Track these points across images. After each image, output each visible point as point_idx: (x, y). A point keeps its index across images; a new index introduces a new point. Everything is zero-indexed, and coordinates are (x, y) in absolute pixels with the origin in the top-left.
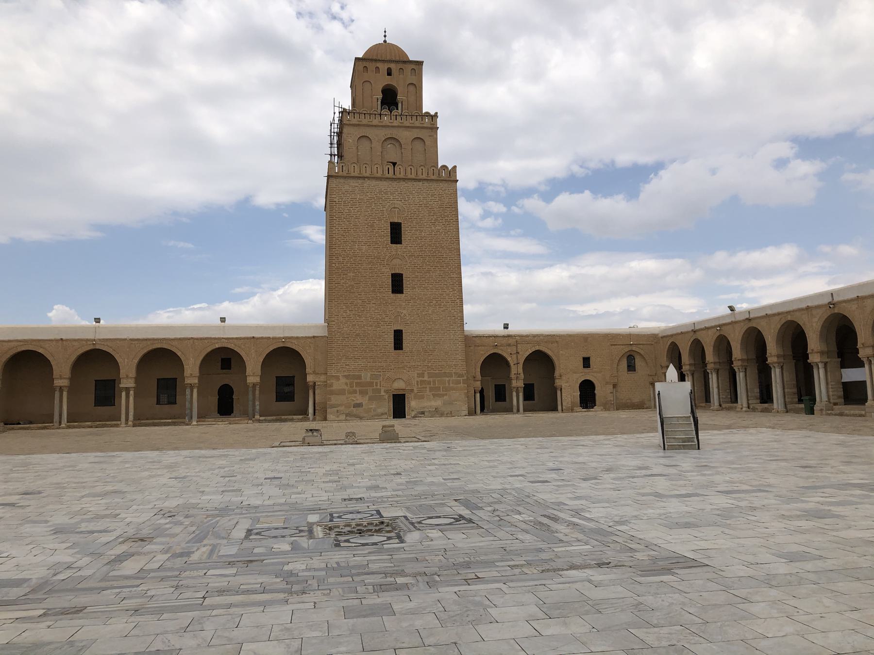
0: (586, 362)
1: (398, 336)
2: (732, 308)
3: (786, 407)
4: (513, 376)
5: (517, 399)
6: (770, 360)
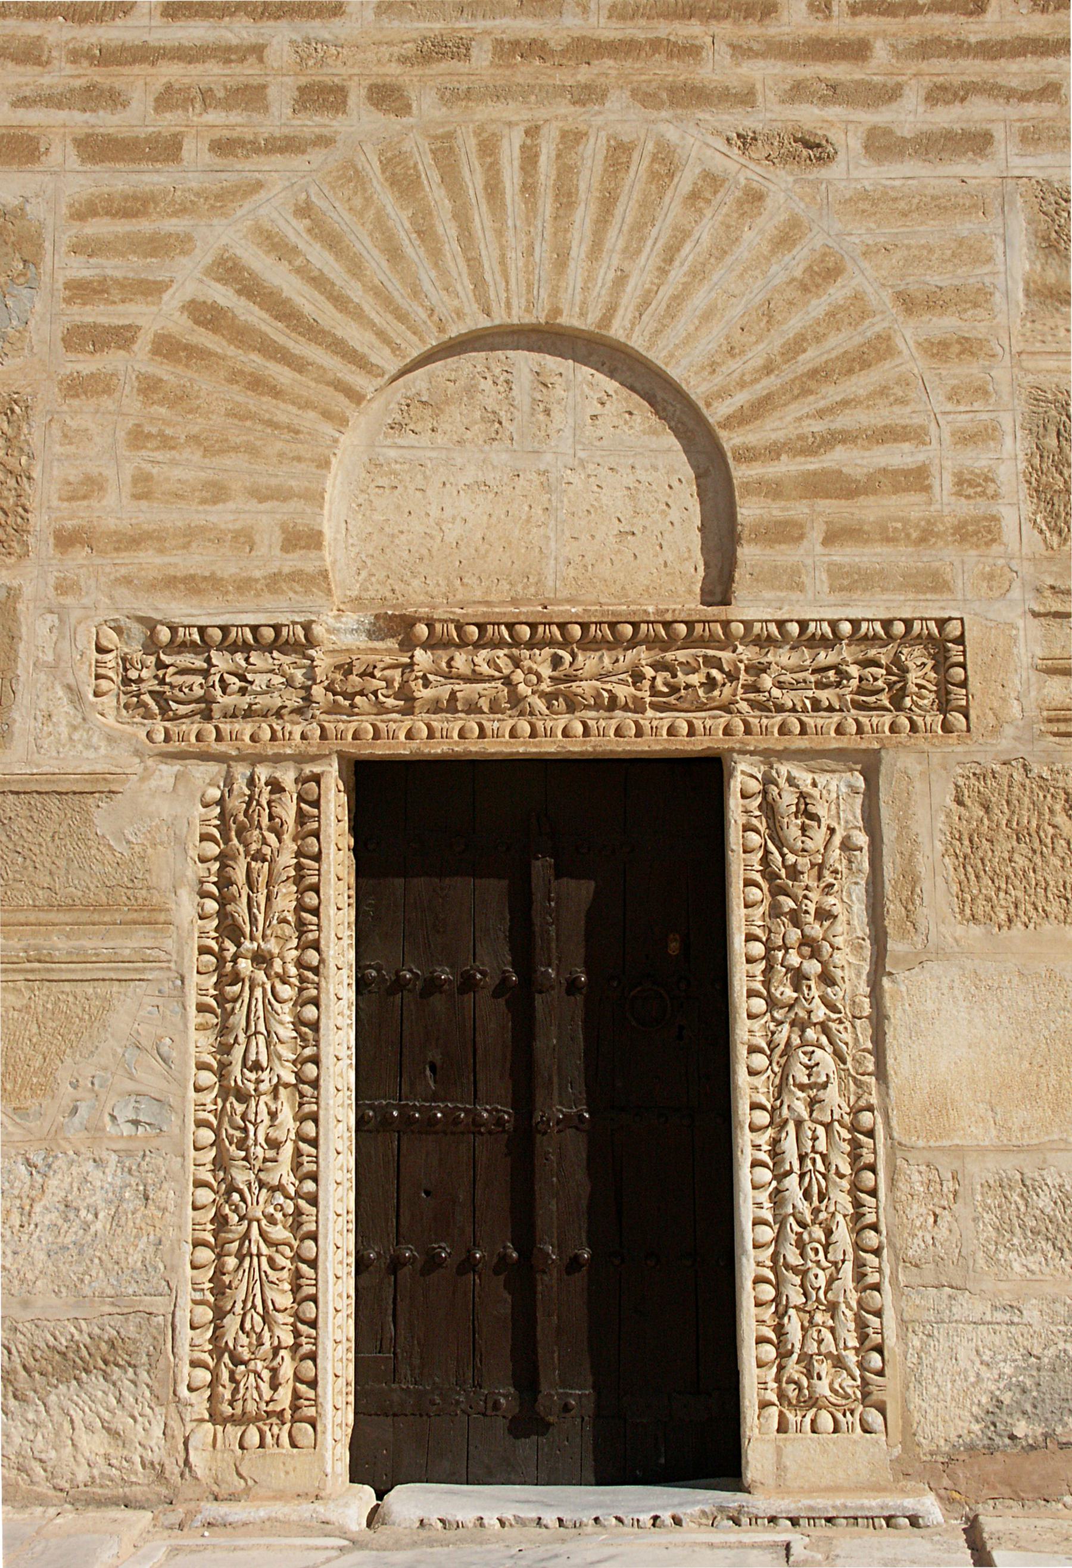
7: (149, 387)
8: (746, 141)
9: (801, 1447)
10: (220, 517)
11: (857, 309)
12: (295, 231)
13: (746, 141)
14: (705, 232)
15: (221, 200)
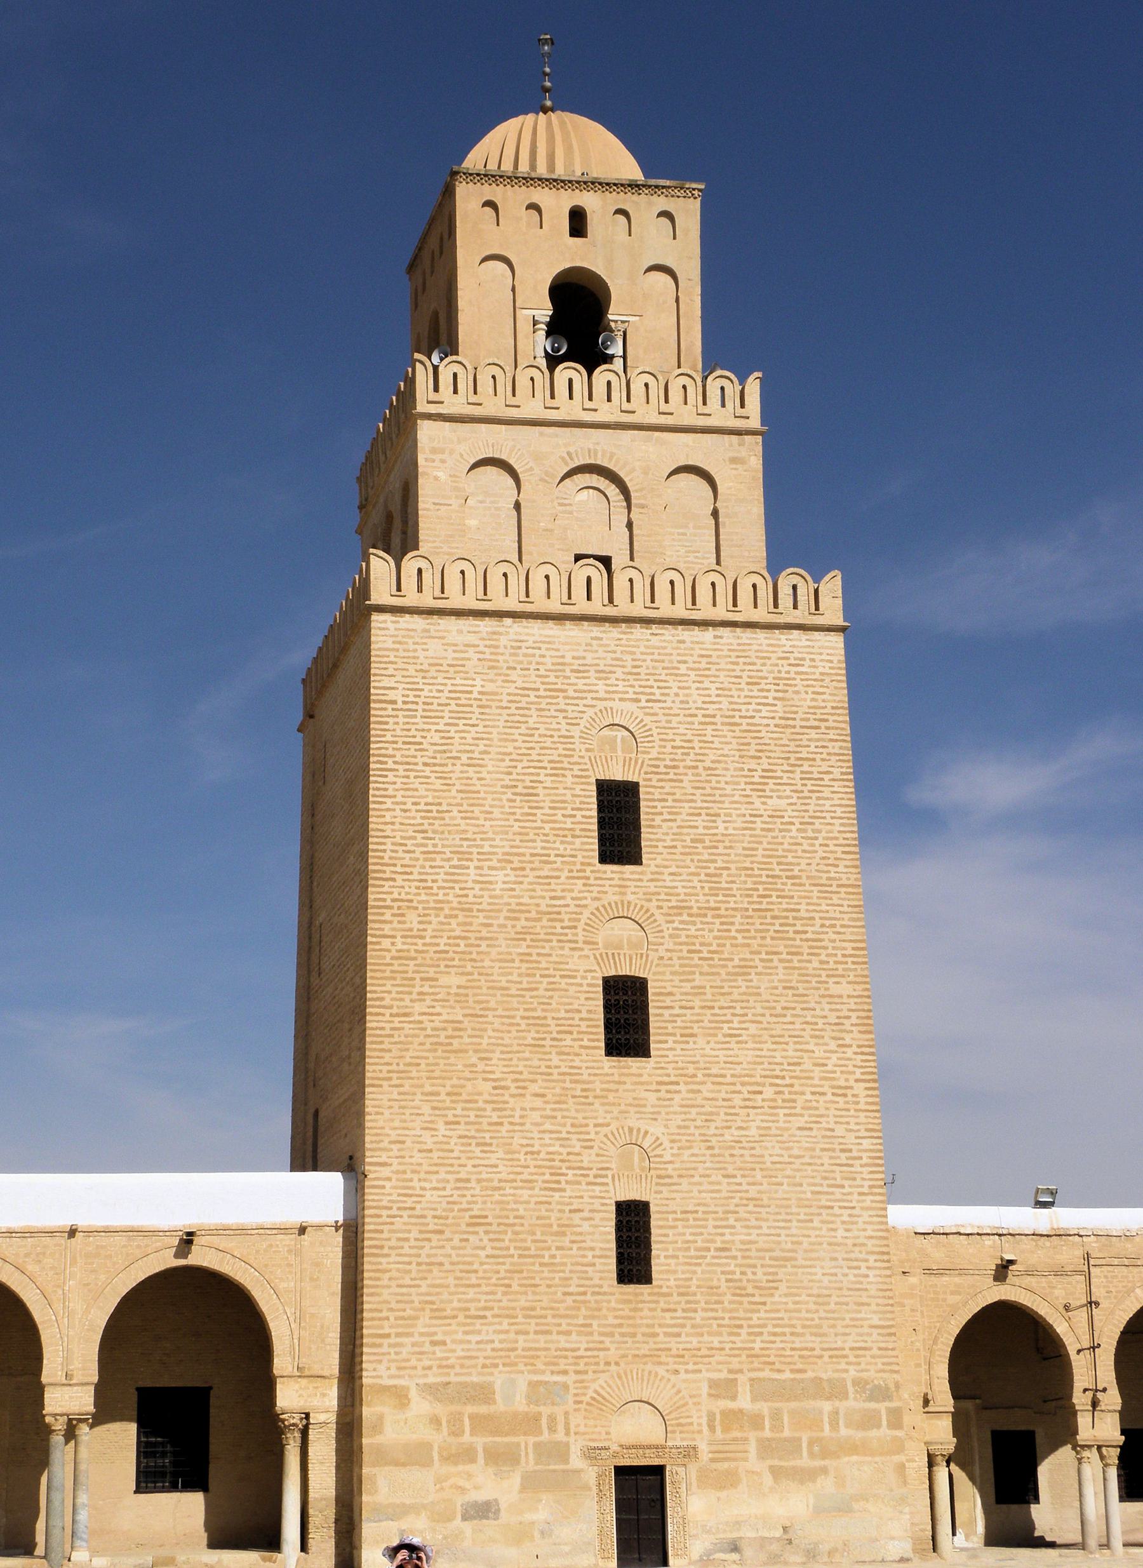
1: (633, 1222)
4: (1080, 1400)
7: (586, 1410)
8: (668, 1371)
9: (677, 1562)
10: (596, 1430)
11: (683, 1398)
12: (605, 1385)
13: (668, 1371)
14: (662, 1385)
15: (594, 1380)
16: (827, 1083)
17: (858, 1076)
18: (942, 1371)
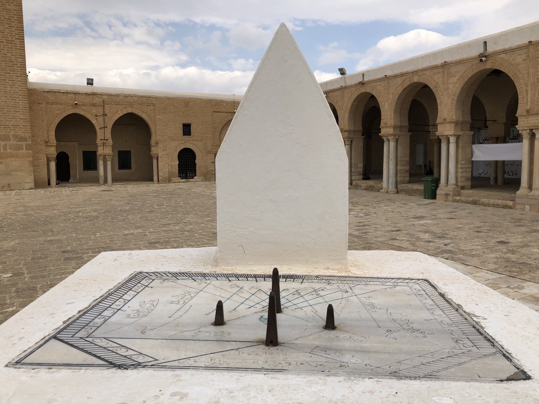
0: (187, 129)
2: (342, 72)
3: (397, 187)
4: (98, 142)
5: (105, 167)
6: (384, 132)
16: (4, 39)
17: (17, 37)
18: (53, 133)
